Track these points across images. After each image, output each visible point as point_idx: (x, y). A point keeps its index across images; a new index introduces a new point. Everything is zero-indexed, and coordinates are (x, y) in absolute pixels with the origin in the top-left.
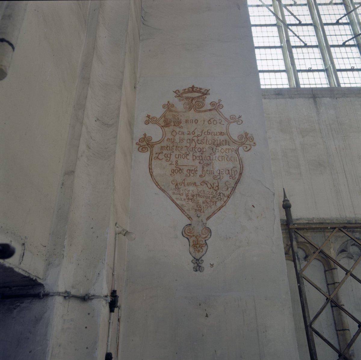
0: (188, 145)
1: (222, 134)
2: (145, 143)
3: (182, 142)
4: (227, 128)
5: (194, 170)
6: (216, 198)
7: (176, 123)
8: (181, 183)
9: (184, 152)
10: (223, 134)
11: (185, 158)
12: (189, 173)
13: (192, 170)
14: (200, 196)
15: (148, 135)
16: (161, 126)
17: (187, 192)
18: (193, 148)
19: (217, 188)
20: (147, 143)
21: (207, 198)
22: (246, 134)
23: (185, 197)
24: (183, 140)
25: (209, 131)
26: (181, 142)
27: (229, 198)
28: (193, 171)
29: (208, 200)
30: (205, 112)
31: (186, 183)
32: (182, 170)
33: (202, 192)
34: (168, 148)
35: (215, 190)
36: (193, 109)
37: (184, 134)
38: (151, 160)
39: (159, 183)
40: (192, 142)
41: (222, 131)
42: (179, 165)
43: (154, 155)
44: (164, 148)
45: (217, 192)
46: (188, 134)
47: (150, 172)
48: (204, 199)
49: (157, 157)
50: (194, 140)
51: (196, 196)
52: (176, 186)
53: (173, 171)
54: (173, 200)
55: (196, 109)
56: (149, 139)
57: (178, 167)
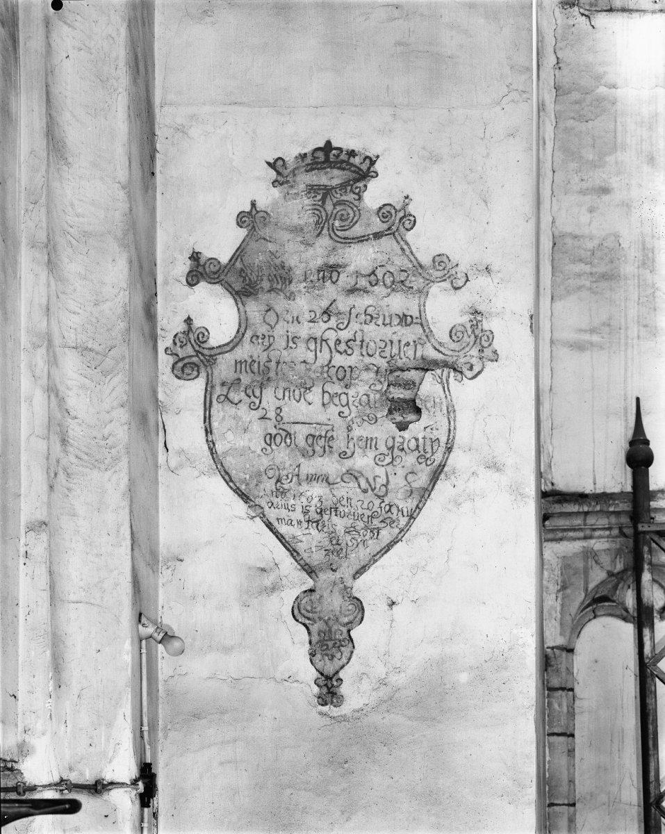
0: (310, 356)
1: (406, 320)
2: (189, 350)
5: (326, 437)
6: (381, 518)
7: (278, 283)
8: (290, 476)
13: (321, 436)
14: (338, 513)
15: (197, 323)
16: (234, 293)
17: (305, 503)
18: (322, 367)
19: (384, 489)
20: (195, 351)
21: (356, 518)
22: (475, 322)
23: (301, 517)
25: (370, 310)
26: (291, 348)
27: (412, 521)
28: (323, 439)
29: (360, 525)
30: (362, 241)
31: (303, 477)
32: (293, 436)
33: (344, 502)
34: (256, 365)
35: (379, 497)
36: (325, 231)
38: (208, 406)
39: (233, 473)
40: (321, 346)
42: (286, 420)
43: (218, 390)
44: (243, 366)
45: (383, 502)
47: (207, 440)
48: (348, 522)
49: (226, 397)
51: (328, 512)
52: (276, 483)
53: (270, 439)
54: (270, 523)
55: (336, 232)
56: (200, 336)
57: (281, 426)
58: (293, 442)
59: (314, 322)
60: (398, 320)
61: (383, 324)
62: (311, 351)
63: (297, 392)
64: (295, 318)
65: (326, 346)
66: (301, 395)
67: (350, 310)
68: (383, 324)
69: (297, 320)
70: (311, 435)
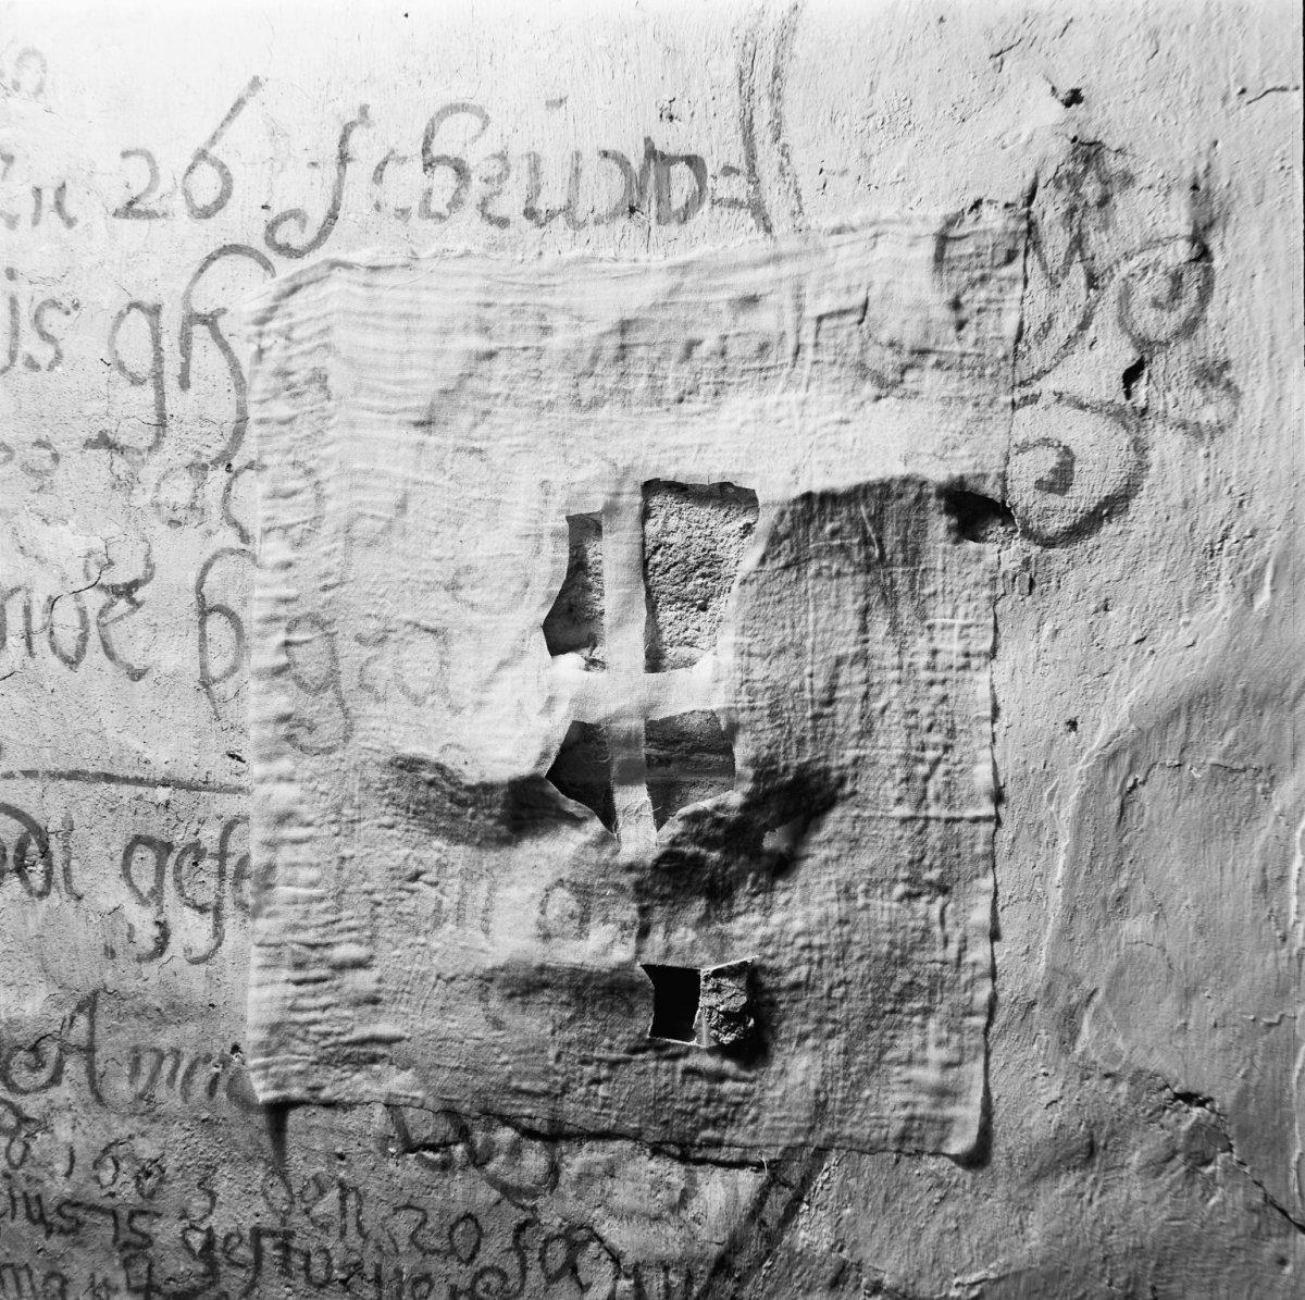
1: (663, 185)
3: (45, 353)
4: (761, 80)
8: (52, 1050)
9: (68, 544)
10: (681, 175)
11: (94, 656)
12: (157, 892)
13: (196, 851)
14: (297, 1260)
18: (199, 469)
22: (1091, 190)
24: (52, 319)
26: (33, 365)
28: (209, 864)
32: (55, 845)
33: (328, 1204)
37: (71, 207)
41: (670, 140)
46: (130, 209)
50: (210, 321)
51: (244, 1253)
58: (58, 873)
59: (150, 215)
60: (618, 180)
61: (530, 213)
62: (136, 381)
63: (66, 614)
64: (49, 198)
65: (214, 350)
66: (84, 623)
67: (344, 140)
68: (530, 213)
69: (59, 206)
70: (149, 842)
